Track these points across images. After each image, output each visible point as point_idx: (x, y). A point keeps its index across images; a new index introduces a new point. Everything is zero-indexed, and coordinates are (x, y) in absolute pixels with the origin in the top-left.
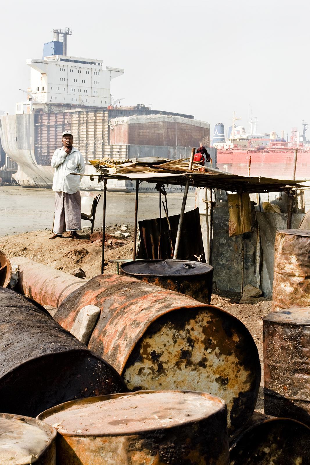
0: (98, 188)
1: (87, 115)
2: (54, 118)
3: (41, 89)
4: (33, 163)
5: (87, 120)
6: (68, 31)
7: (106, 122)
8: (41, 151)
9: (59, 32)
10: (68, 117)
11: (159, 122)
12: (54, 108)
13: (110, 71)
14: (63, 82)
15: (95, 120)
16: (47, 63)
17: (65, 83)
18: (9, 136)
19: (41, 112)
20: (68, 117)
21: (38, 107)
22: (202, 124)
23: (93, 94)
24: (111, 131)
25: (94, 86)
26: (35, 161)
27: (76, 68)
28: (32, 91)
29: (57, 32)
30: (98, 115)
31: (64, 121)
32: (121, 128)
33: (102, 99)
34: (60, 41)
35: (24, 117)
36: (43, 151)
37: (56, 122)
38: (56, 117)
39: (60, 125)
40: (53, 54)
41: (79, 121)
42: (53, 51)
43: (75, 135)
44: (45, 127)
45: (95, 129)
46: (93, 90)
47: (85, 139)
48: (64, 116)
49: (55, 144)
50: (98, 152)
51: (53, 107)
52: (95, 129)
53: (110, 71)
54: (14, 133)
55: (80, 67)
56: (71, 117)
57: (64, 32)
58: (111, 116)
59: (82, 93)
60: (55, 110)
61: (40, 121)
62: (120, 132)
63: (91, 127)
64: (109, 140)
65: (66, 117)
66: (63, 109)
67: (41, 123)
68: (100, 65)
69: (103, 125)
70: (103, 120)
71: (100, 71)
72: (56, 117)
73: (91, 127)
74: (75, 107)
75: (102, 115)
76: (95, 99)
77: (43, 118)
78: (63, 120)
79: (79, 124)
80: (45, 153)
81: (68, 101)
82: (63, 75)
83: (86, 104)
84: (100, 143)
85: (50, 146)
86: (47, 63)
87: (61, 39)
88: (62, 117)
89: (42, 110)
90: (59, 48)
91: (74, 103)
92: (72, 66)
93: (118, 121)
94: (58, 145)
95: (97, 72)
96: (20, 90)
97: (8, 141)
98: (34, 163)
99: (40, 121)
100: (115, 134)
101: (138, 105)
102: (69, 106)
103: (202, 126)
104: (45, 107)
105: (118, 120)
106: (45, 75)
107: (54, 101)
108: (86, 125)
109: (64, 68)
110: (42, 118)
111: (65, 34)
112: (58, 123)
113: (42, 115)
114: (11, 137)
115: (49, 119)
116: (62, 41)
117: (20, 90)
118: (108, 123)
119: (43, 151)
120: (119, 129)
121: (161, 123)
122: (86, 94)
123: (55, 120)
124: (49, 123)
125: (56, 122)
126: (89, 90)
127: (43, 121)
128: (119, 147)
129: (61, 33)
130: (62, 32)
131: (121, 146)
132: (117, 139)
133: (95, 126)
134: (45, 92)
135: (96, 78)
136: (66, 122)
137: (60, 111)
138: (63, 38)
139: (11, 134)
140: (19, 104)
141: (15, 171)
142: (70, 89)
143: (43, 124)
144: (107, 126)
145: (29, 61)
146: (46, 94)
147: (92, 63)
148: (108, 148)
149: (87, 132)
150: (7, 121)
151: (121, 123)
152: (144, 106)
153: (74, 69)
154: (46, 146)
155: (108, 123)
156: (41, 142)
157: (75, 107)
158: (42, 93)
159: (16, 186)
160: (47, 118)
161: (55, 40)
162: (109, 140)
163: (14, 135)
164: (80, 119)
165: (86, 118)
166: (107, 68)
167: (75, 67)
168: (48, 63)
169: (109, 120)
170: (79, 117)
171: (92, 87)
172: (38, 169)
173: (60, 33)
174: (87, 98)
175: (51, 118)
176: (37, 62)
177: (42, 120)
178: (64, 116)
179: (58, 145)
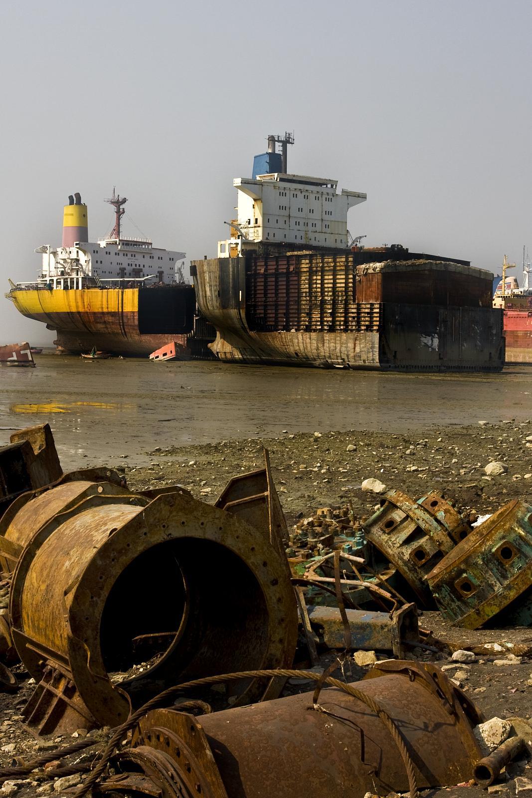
0: (339, 365)
1: (323, 259)
2: (274, 263)
3: (253, 222)
4: (242, 327)
5: (323, 267)
6: (289, 138)
7: (351, 270)
8: (255, 310)
9: (276, 139)
10: (294, 262)
11: (425, 270)
12: (271, 249)
13: (348, 196)
14: (283, 212)
15: (335, 266)
16: (262, 185)
17: (286, 213)
18: (208, 289)
19: (254, 256)
20: (294, 262)
21: (249, 248)
22: (482, 274)
23: (324, 230)
24: (357, 284)
25: (326, 217)
26: (246, 325)
27: (301, 192)
28: (240, 225)
29: (272, 140)
30: (338, 260)
31: (288, 268)
32: (372, 279)
33: (337, 237)
34: (277, 152)
35: (231, 262)
36: (258, 311)
37: (277, 269)
38: (277, 262)
39: (283, 273)
40: (268, 171)
41: (310, 268)
42: (267, 167)
43: (304, 288)
44: (261, 276)
45: (335, 279)
46: (325, 223)
47: (320, 294)
48: (288, 262)
49: (275, 301)
50: (339, 313)
51: (270, 248)
52: (335, 279)
53: (348, 196)
54: (216, 285)
55: (307, 190)
56: (299, 263)
57: (283, 139)
58: (358, 262)
59: (310, 228)
60: (273, 252)
61: (254, 268)
62: (371, 285)
63: (329, 278)
64: (354, 296)
65: (291, 262)
66: (284, 250)
67: (256, 270)
68: (334, 187)
69: (347, 275)
70: (347, 266)
71: (333, 196)
72: (277, 262)
73: (329, 278)
74: (301, 247)
75: (344, 260)
76: (327, 236)
77: (258, 264)
78: (287, 266)
79: (311, 272)
80: (260, 313)
81: (290, 239)
82: (284, 201)
83: (313, 243)
84: (342, 301)
85: (268, 303)
86: (262, 185)
87: (279, 149)
88: (285, 262)
89: (254, 251)
90: (277, 163)
91: (298, 241)
92: (295, 189)
93: (367, 269)
94: (279, 303)
95: (330, 197)
96: (225, 222)
97: (206, 297)
98: (244, 328)
99: (254, 268)
100: (363, 288)
101: (393, 246)
102: (292, 247)
103: (482, 277)
104: (259, 248)
105: (367, 267)
106: (259, 202)
107: (272, 240)
108: (320, 274)
109: (286, 191)
110: (256, 263)
111: (286, 142)
112: (280, 271)
113: (256, 259)
114: (211, 290)
115: (266, 265)
116: (281, 153)
117: (225, 222)
118: (354, 272)
119: (258, 311)
120: (370, 281)
121: (426, 272)
122: (314, 229)
123: (275, 267)
124: (266, 270)
125: (277, 269)
126: (319, 224)
127: (258, 268)
128: (369, 306)
129: (279, 141)
130: (280, 139)
131: (372, 305)
132: (366, 294)
133: (335, 275)
134: (259, 227)
135: (328, 206)
136: (291, 269)
137: (280, 253)
138: (281, 148)
139: (210, 286)
140: (223, 242)
141: (212, 339)
142: (293, 221)
143: (258, 271)
144: (351, 276)
145: (238, 182)
146: (260, 230)
147: (321, 185)
148: (353, 308)
149: (322, 284)
150: (205, 268)
151: (373, 272)
152: (402, 247)
153: (299, 193)
154: (274, 303)
155: (354, 272)
156: (254, 297)
157: (301, 247)
158: (255, 227)
159: (213, 360)
160: (263, 264)
161: (270, 151)
162: (354, 296)
163: (215, 288)
164: (311, 265)
165: (321, 265)
166: (343, 191)
167: (300, 190)
168: (263, 184)
169: (354, 267)
170: (311, 263)
171: (322, 220)
172: (250, 336)
173: (277, 141)
174: (317, 235)
175: (270, 263)
176: (248, 183)
177: (256, 266)
178: (288, 262)
179: (279, 303)
